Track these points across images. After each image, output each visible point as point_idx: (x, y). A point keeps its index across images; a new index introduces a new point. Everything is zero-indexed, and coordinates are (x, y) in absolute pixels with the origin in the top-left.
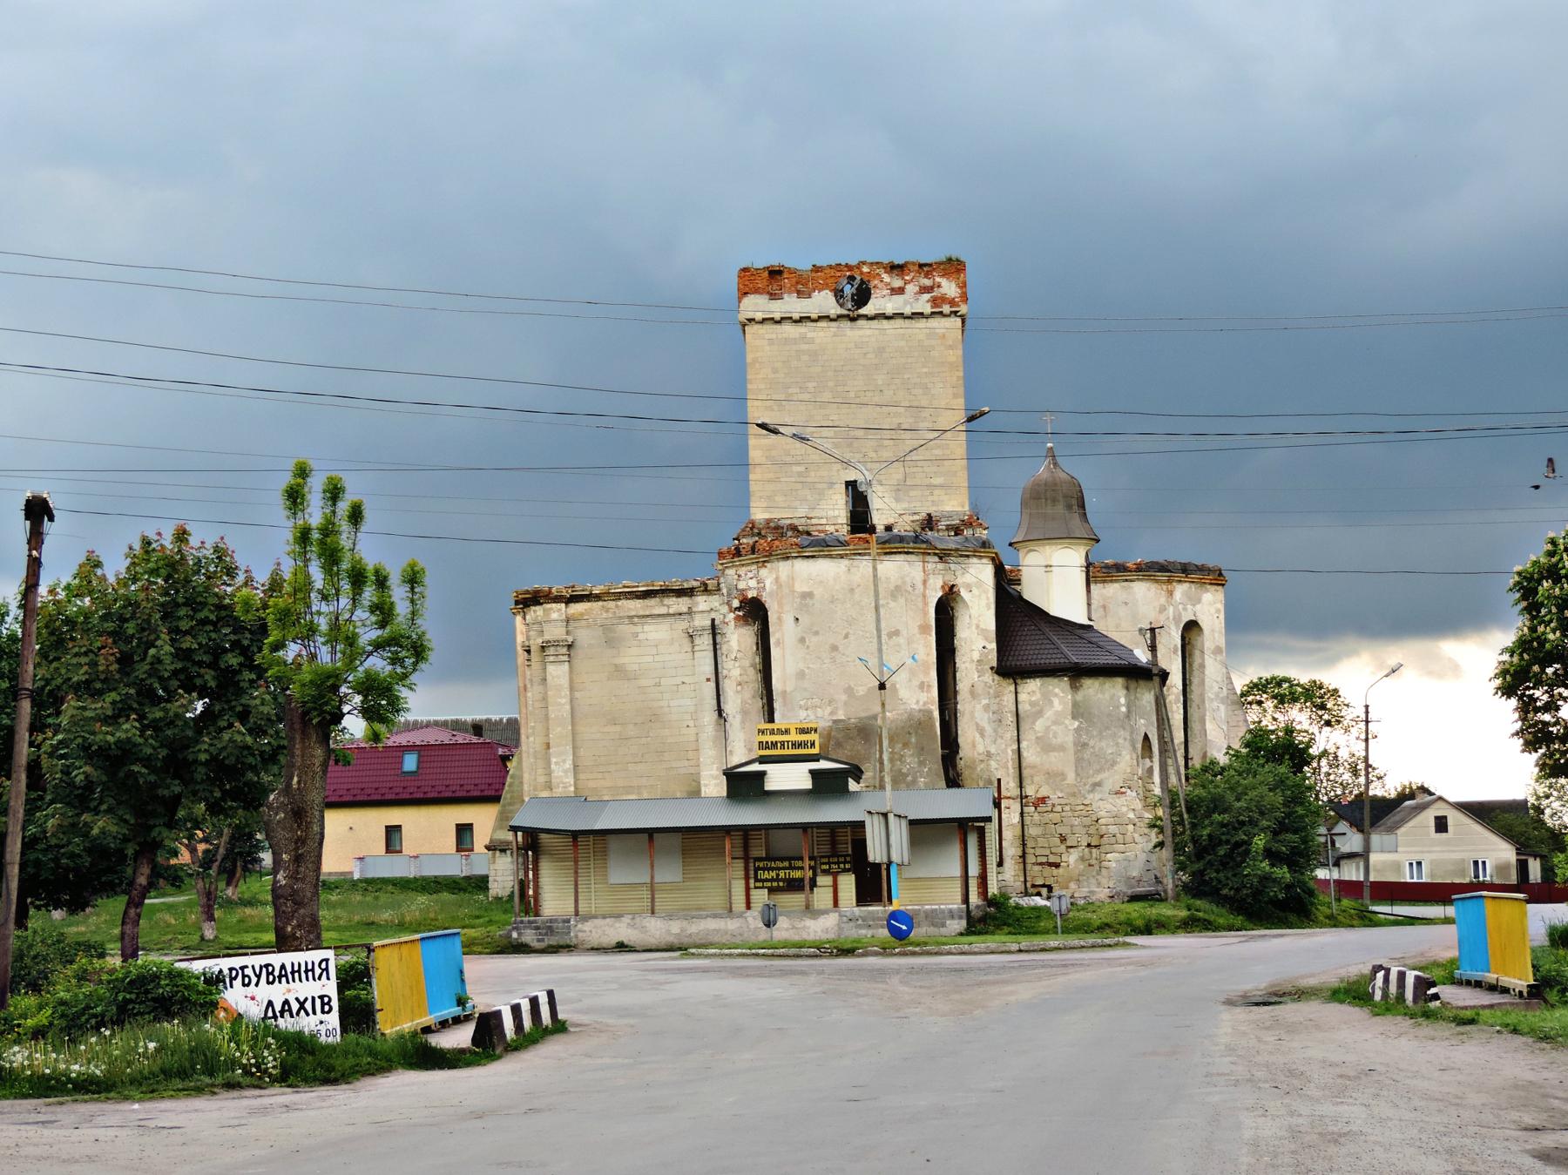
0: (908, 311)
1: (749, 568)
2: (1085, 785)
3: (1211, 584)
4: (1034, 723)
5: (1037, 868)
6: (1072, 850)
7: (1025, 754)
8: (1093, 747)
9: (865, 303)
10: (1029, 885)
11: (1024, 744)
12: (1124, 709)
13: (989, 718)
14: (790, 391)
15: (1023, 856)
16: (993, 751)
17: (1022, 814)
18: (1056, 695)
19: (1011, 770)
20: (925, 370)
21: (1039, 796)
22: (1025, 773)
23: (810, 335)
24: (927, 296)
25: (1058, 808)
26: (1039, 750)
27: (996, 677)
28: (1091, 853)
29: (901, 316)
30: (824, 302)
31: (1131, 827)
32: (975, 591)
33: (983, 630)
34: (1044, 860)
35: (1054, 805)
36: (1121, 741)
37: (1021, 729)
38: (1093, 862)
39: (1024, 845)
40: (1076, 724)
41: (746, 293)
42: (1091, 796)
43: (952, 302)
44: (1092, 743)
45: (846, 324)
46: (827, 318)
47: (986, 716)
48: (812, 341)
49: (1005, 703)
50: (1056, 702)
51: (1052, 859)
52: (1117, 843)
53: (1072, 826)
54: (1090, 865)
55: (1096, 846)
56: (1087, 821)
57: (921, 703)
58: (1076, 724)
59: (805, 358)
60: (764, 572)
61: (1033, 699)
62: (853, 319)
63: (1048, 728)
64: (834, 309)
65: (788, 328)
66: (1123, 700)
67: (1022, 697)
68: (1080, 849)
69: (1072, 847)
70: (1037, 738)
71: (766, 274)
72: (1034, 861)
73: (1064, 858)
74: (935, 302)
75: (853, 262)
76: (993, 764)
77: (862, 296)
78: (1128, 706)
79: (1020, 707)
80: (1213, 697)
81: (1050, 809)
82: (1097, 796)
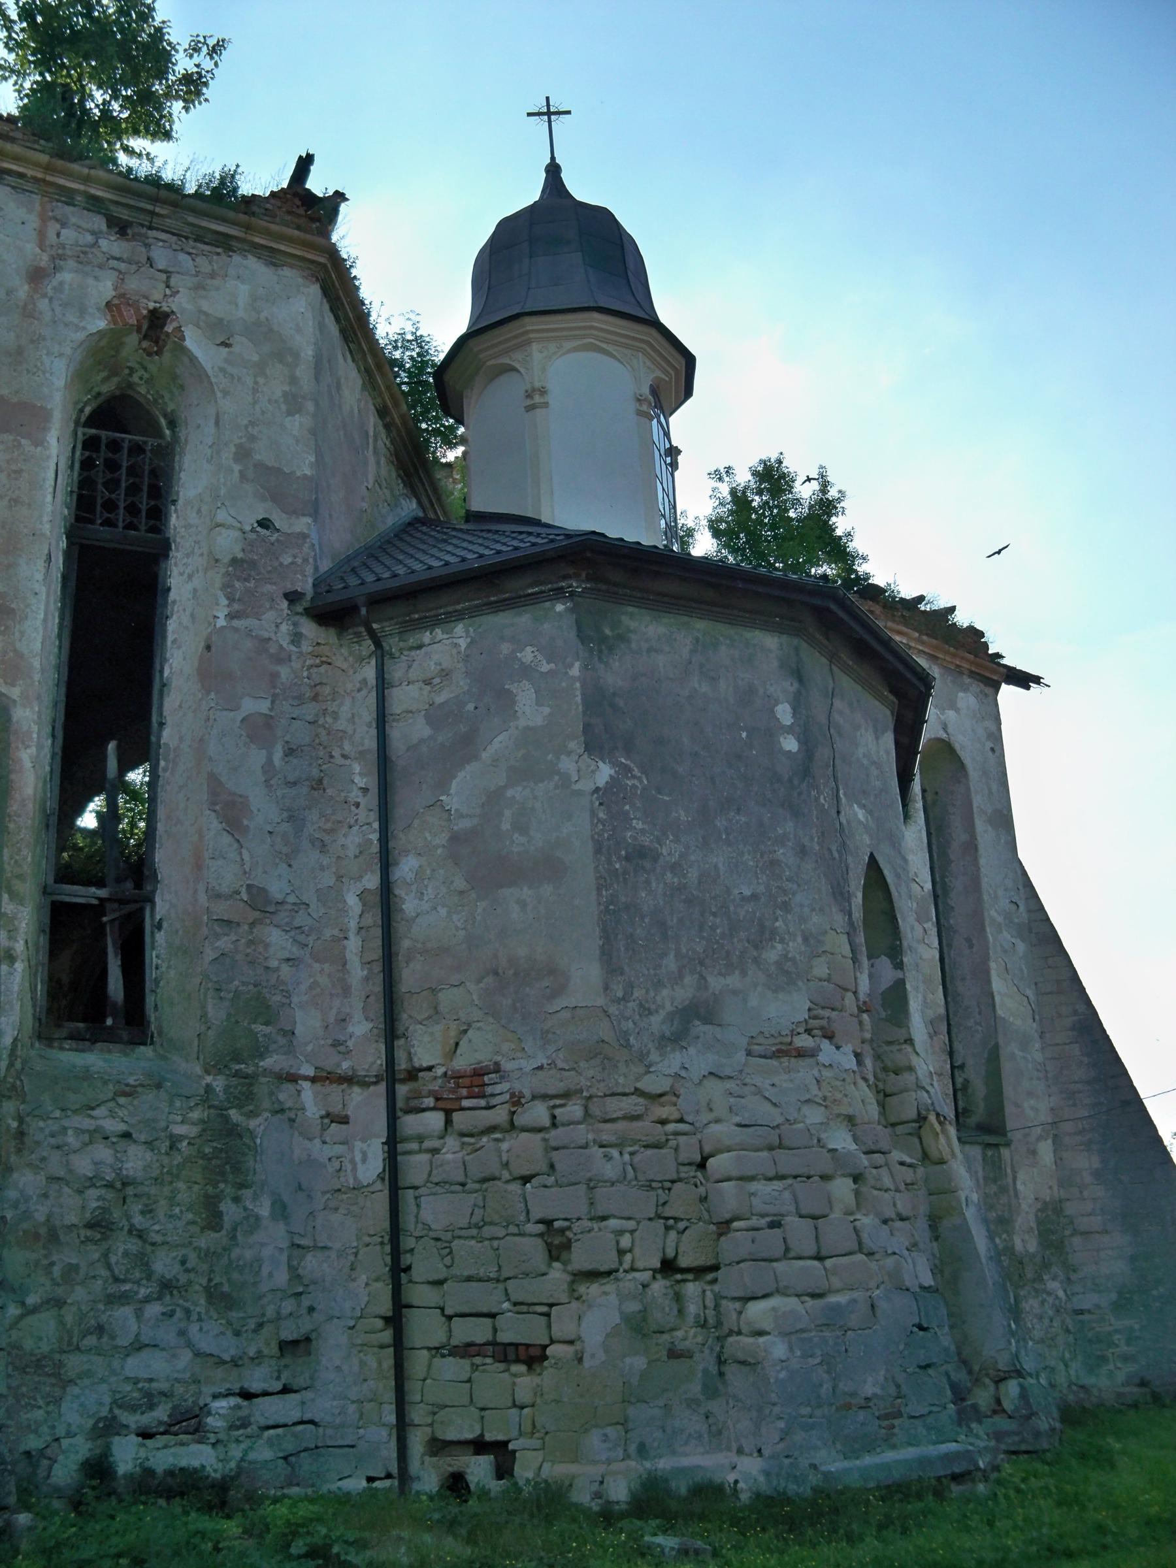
2: (646, 1011)
4: (442, 785)
5: (453, 1368)
6: (593, 1289)
7: (409, 904)
8: (674, 868)
10: (417, 1443)
11: (406, 868)
12: (790, 744)
13: (268, 767)
15: (396, 1320)
16: (276, 888)
17: (393, 1142)
18: (526, 672)
19: (357, 972)
21: (463, 1062)
22: (409, 976)
25: (538, 1113)
26: (460, 883)
27: (309, 628)
28: (678, 1297)
31: (842, 1188)
32: (242, 345)
33: (260, 466)
34: (478, 1332)
35: (516, 1100)
37: (400, 813)
38: (688, 1336)
39: (398, 1271)
40: (604, 773)
42: (674, 1061)
44: (670, 850)
47: (257, 757)
49: (342, 724)
50: (525, 696)
51: (514, 1329)
52: (787, 1254)
53: (592, 1185)
54: (674, 1354)
55: (700, 1272)
56: (661, 1164)
58: (604, 773)
61: (439, 699)
63: (494, 798)
66: (784, 713)
67: (403, 697)
68: (630, 1282)
69: (593, 1275)
70: (455, 838)
72: (438, 1336)
73: (563, 1325)
76: (278, 941)
79: (396, 733)
80: (1000, 919)
81: (499, 1115)
82: (697, 1060)
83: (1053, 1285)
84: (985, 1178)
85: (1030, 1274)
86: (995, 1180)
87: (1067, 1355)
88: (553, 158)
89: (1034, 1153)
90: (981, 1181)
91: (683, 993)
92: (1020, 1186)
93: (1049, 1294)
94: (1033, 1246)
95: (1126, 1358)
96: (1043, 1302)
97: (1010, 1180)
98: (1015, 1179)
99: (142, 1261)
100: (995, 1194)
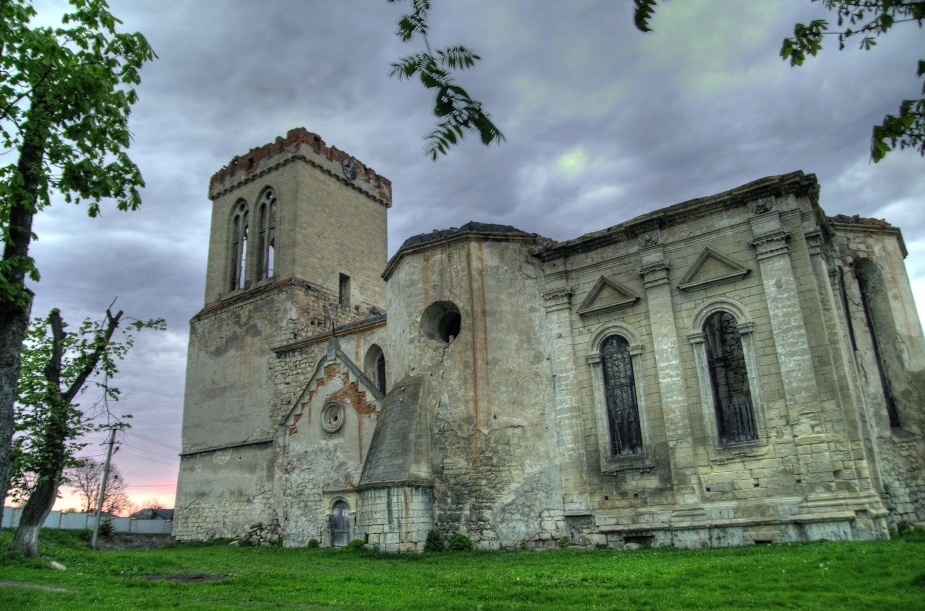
1: (856, 234)
14: (318, 208)
23: (328, 182)
24: (378, 190)
29: (367, 194)
30: (335, 167)
41: (303, 141)
45: (344, 187)
46: (337, 178)
48: (328, 186)
59: (325, 193)
60: (870, 241)
62: (347, 184)
64: (341, 175)
65: (318, 173)
71: (312, 137)
75: (351, 156)
77: (354, 176)
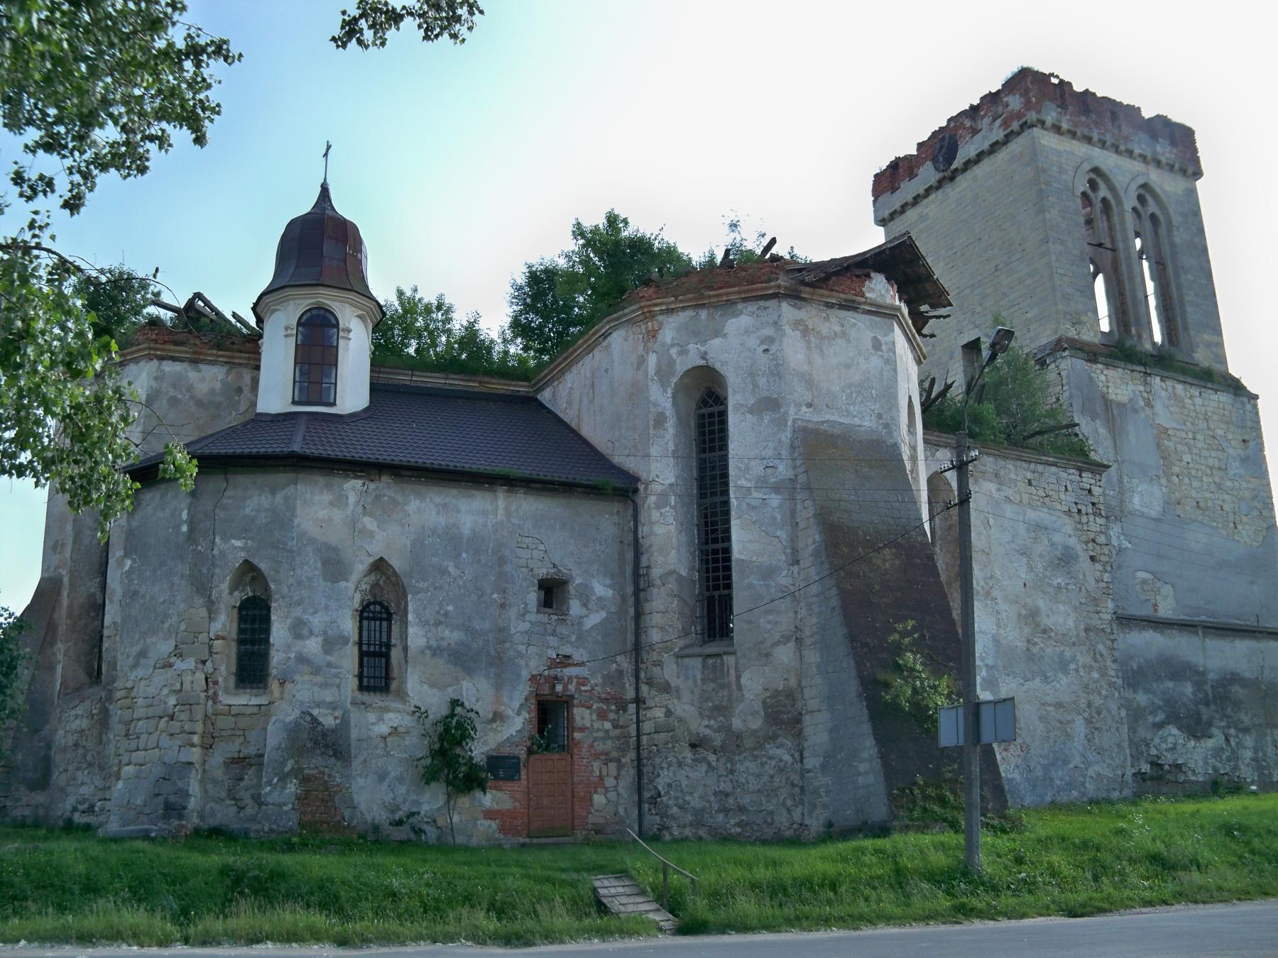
0: (986, 146)
2: (128, 656)
3: (745, 300)
9: (954, 158)
12: (185, 528)
20: (1011, 198)
36: (176, 580)
43: (1019, 115)
57: (52, 569)
74: (1005, 124)
78: (192, 523)
83: (778, 751)
84: (703, 680)
85: (749, 743)
86: (714, 680)
87: (789, 803)
88: (325, 179)
89: (768, 655)
90: (699, 681)
91: (136, 649)
92: (743, 681)
93: (771, 758)
94: (756, 723)
95: (825, 806)
96: (763, 764)
97: (733, 679)
98: (738, 677)
99: (85, 756)
100: (714, 690)
